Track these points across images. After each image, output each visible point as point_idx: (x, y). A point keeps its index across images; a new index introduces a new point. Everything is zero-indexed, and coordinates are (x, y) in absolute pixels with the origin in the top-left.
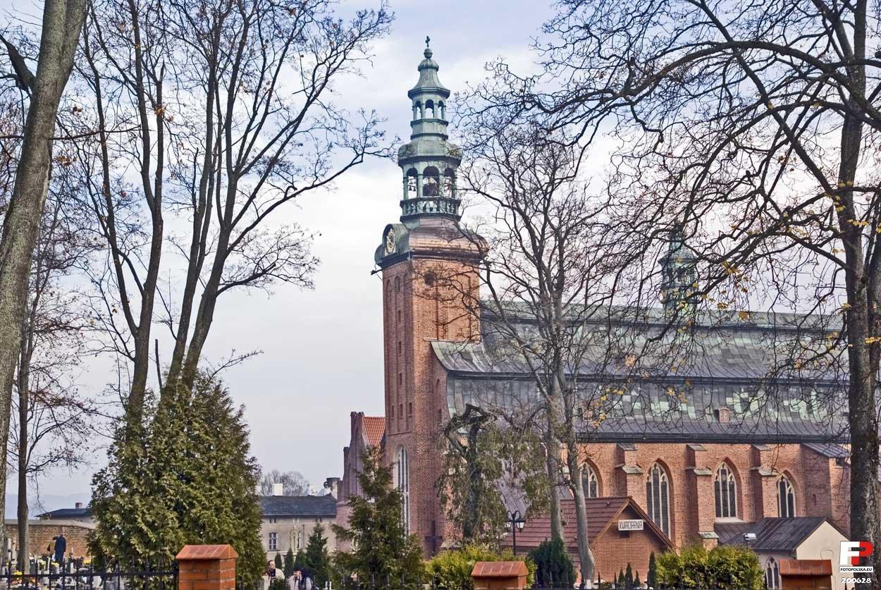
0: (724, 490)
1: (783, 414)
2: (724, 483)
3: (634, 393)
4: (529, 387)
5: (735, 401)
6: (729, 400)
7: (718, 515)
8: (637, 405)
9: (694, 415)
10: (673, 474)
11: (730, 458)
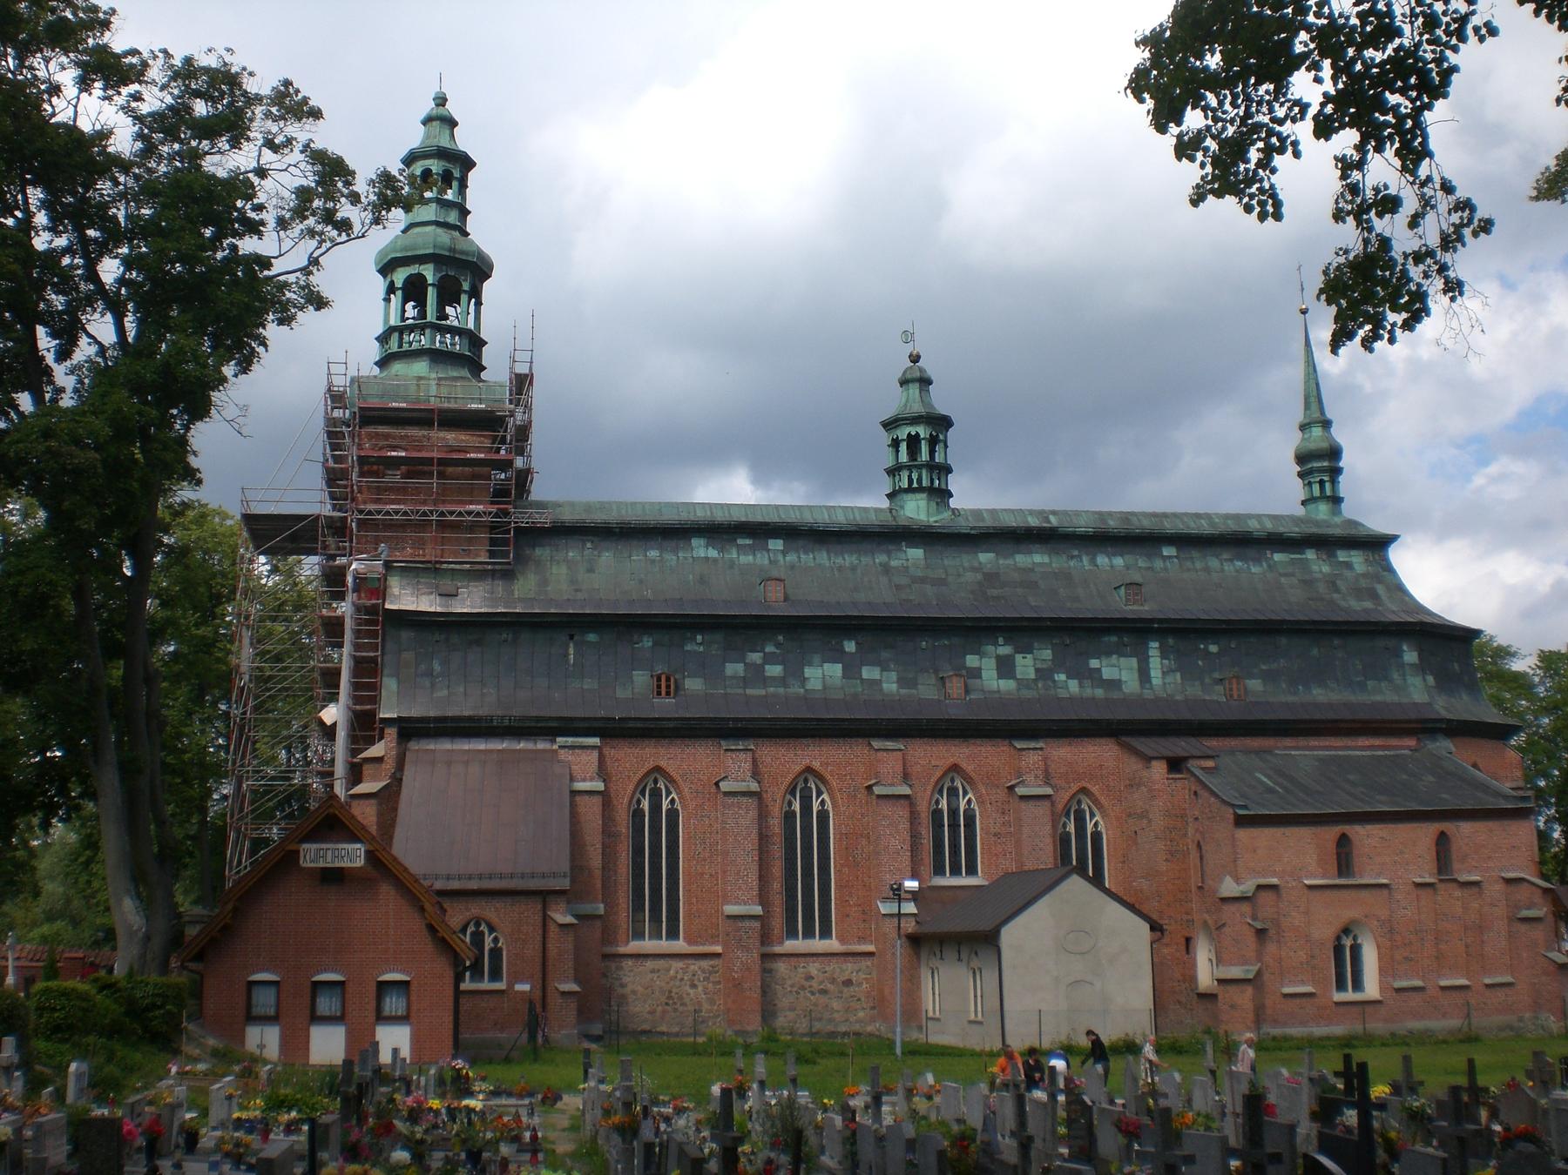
0: (954, 826)
2: (953, 812)
3: (770, 649)
5: (984, 664)
6: (972, 661)
7: (939, 870)
8: (775, 670)
9: (894, 687)
11: (964, 765)
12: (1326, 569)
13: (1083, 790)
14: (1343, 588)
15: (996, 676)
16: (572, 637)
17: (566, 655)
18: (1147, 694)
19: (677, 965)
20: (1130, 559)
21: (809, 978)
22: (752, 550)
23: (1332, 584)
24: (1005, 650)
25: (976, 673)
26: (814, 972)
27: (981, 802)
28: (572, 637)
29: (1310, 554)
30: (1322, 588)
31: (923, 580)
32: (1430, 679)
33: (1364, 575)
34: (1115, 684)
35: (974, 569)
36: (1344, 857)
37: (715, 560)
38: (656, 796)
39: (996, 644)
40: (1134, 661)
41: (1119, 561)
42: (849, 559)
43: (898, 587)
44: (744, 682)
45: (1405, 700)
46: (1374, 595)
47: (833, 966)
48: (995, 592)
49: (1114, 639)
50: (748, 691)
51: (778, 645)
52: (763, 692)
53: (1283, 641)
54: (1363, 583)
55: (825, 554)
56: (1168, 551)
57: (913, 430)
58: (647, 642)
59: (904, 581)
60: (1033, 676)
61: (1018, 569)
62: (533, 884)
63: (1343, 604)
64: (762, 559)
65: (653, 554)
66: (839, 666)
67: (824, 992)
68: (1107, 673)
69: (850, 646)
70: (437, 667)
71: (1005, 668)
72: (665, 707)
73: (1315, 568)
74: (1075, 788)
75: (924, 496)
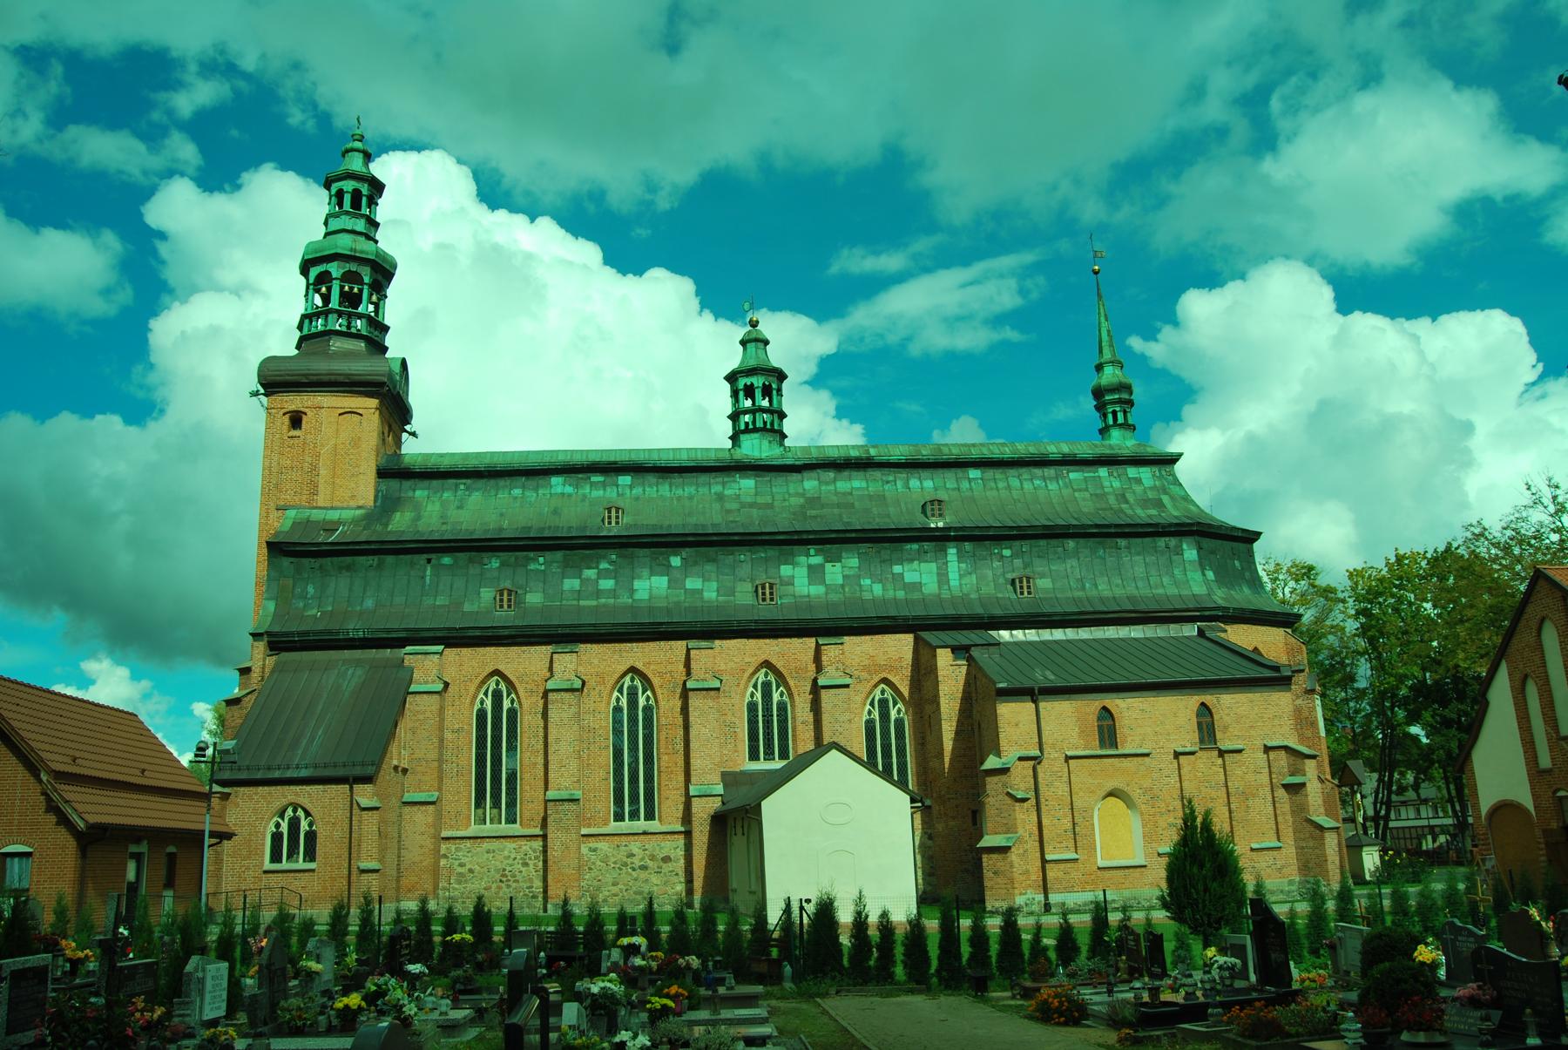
1: (890, 586)
3: (604, 565)
4: (412, 564)
6: (786, 570)
8: (607, 584)
9: (714, 595)
10: (659, 691)
11: (774, 662)
12: (1116, 484)
13: (885, 681)
14: (1131, 500)
15: (804, 581)
16: (429, 561)
17: (423, 578)
18: (945, 595)
19: (510, 845)
20: (939, 482)
21: (631, 855)
22: (604, 485)
23: (1122, 497)
24: (816, 560)
25: (790, 582)
26: (635, 850)
27: (791, 695)
28: (429, 561)
29: (1103, 472)
30: (1112, 500)
31: (752, 505)
32: (1210, 575)
33: (1151, 488)
34: (917, 586)
35: (797, 495)
36: (1108, 731)
37: (570, 495)
38: (497, 697)
39: (808, 555)
40: (933, 566)
41: (928, 484)
42: (690, 490)
43: (729, 512)
44: (579, 594)
45: (1185, 592)
46: (1159, 504)
47: (651, 844)
48: (813, 513)
49: (915, 546)
50: (582, 603)
51: (611, 563)
52: (594, 603)
53: (1071, 544)
54: (1151, 495)
55: (667, 487)
56: (974, 473)
57: (748, 381)
58: (495, 563)
59: (734, 506)
60: (840, 581)
61: (836, 493)
62: (341, 772)
63: (1130, 512)
64: (611, 493)
65: (517, 492)
66: (665, 579)
67: (643, 868)
68: (910, 577)
69: (676, 561)
70: (311, 589)
71: (816, 573)
72: (504, 617)
73: (1106, 484)
74: (877, 679)
75: (756, 435)
